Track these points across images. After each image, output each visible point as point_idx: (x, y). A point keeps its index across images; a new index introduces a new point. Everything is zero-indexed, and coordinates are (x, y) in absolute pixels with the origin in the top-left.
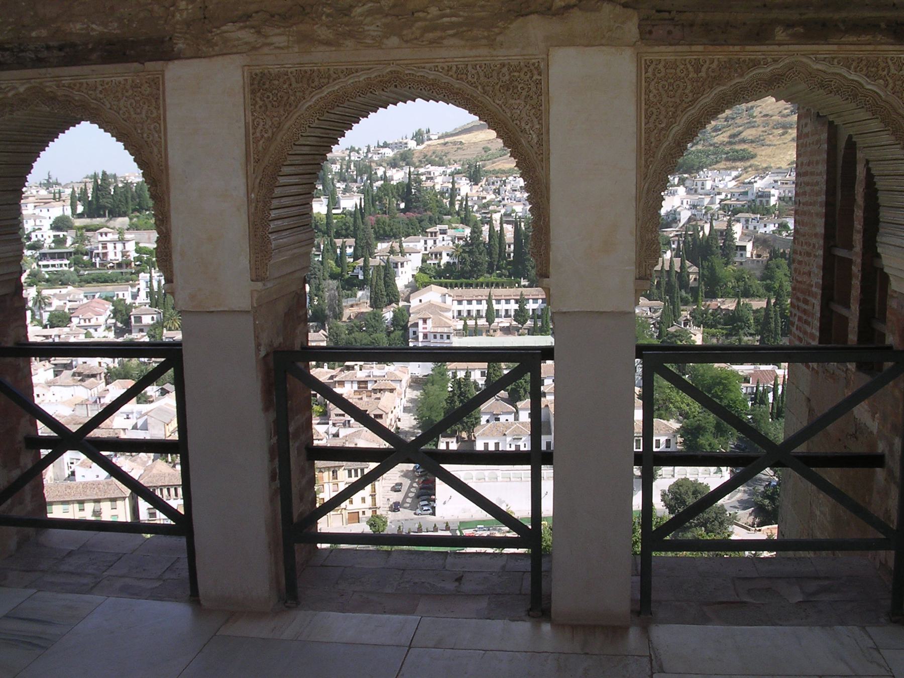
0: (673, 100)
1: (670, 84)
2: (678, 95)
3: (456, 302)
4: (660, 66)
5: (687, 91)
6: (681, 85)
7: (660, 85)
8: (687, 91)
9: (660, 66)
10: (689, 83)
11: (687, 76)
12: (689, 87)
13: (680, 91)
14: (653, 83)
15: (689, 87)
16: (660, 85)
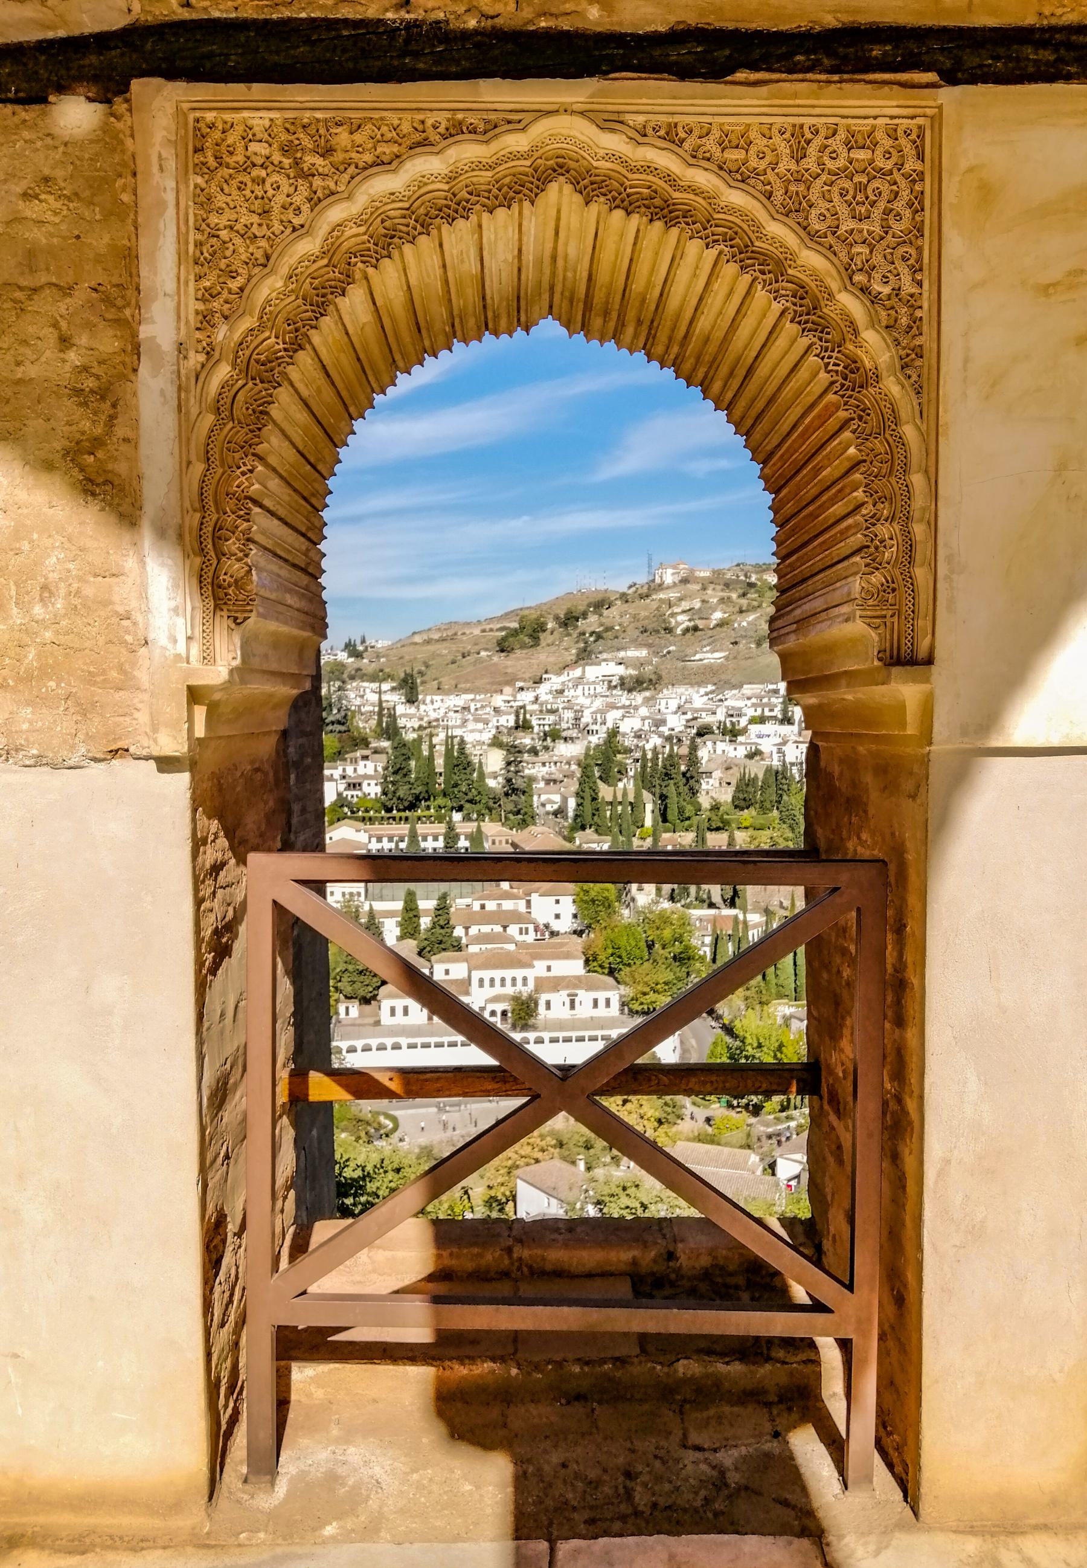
0: (865, 226)
1: (861, 188)
2: (877, 213)
3: (374, 840)
4: (836, 143)
5: (899, 205)
6: (885, 188)
7: (836, 190)
8: (899, 205)
9: (836, 143)
10: (903, 183)
11: (900, 166)
12: (905, 194)
13: (882, 205)
14: (819, 182)
15: (905, 194)
16: (836, 190)
